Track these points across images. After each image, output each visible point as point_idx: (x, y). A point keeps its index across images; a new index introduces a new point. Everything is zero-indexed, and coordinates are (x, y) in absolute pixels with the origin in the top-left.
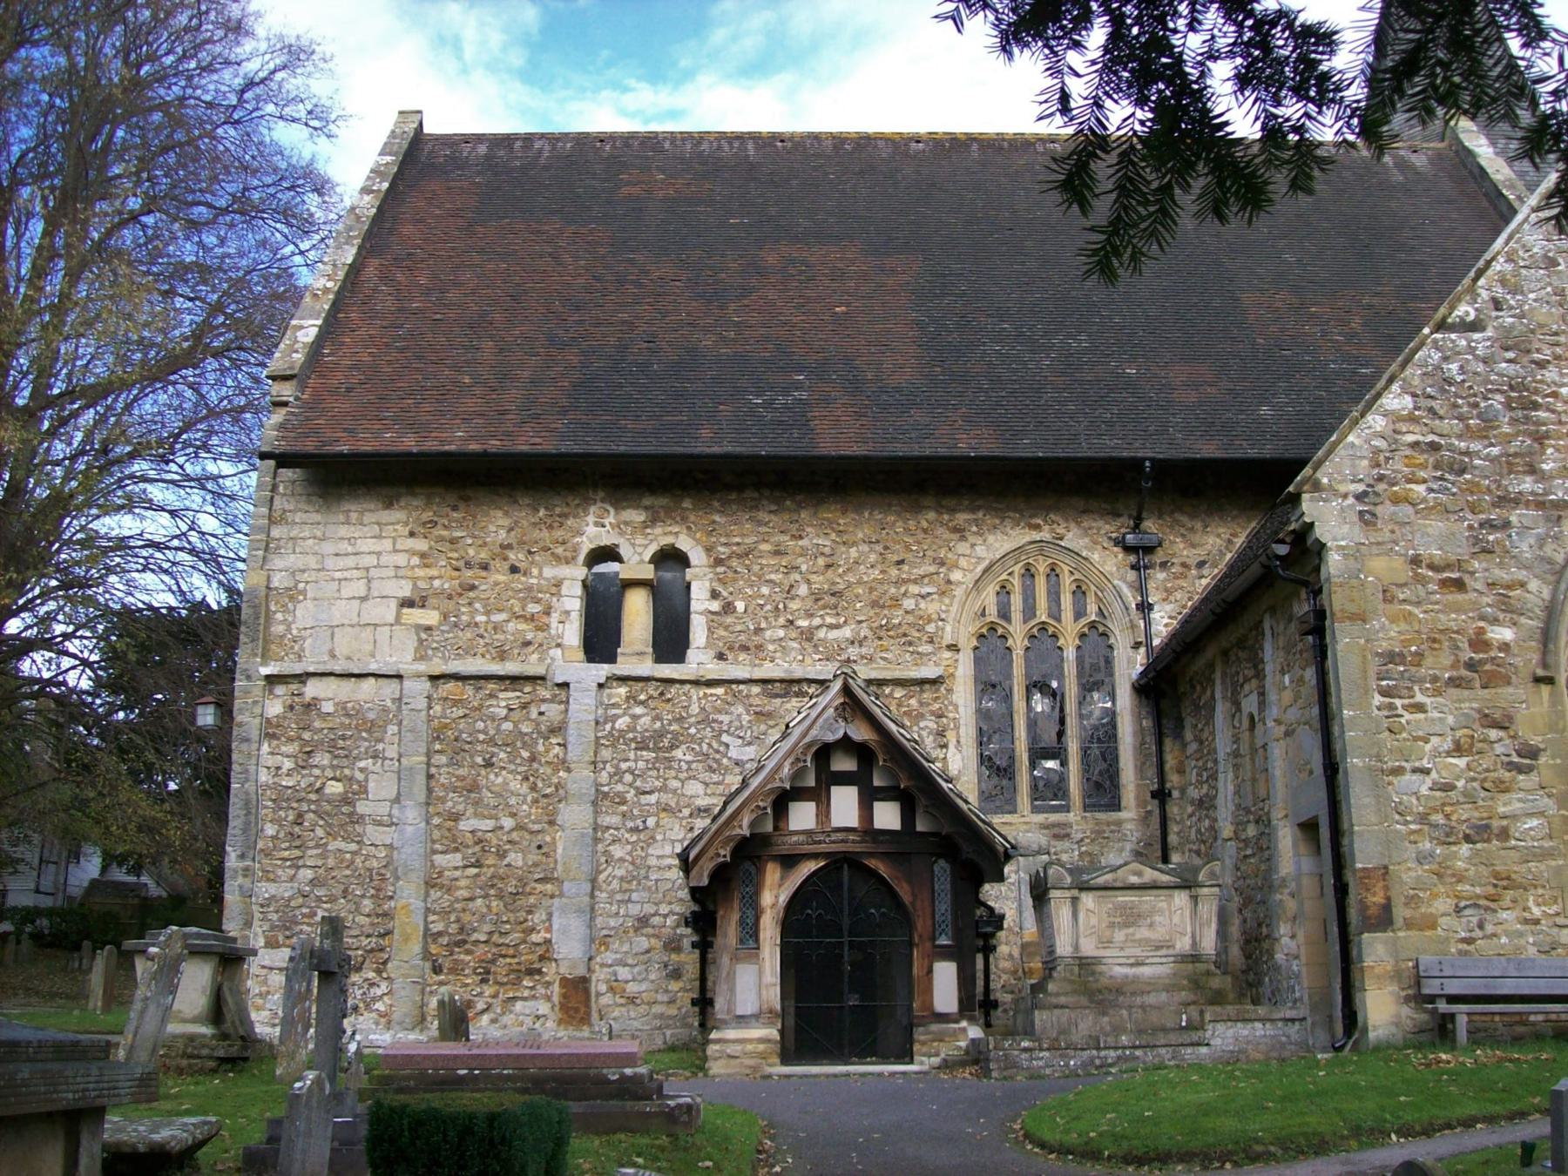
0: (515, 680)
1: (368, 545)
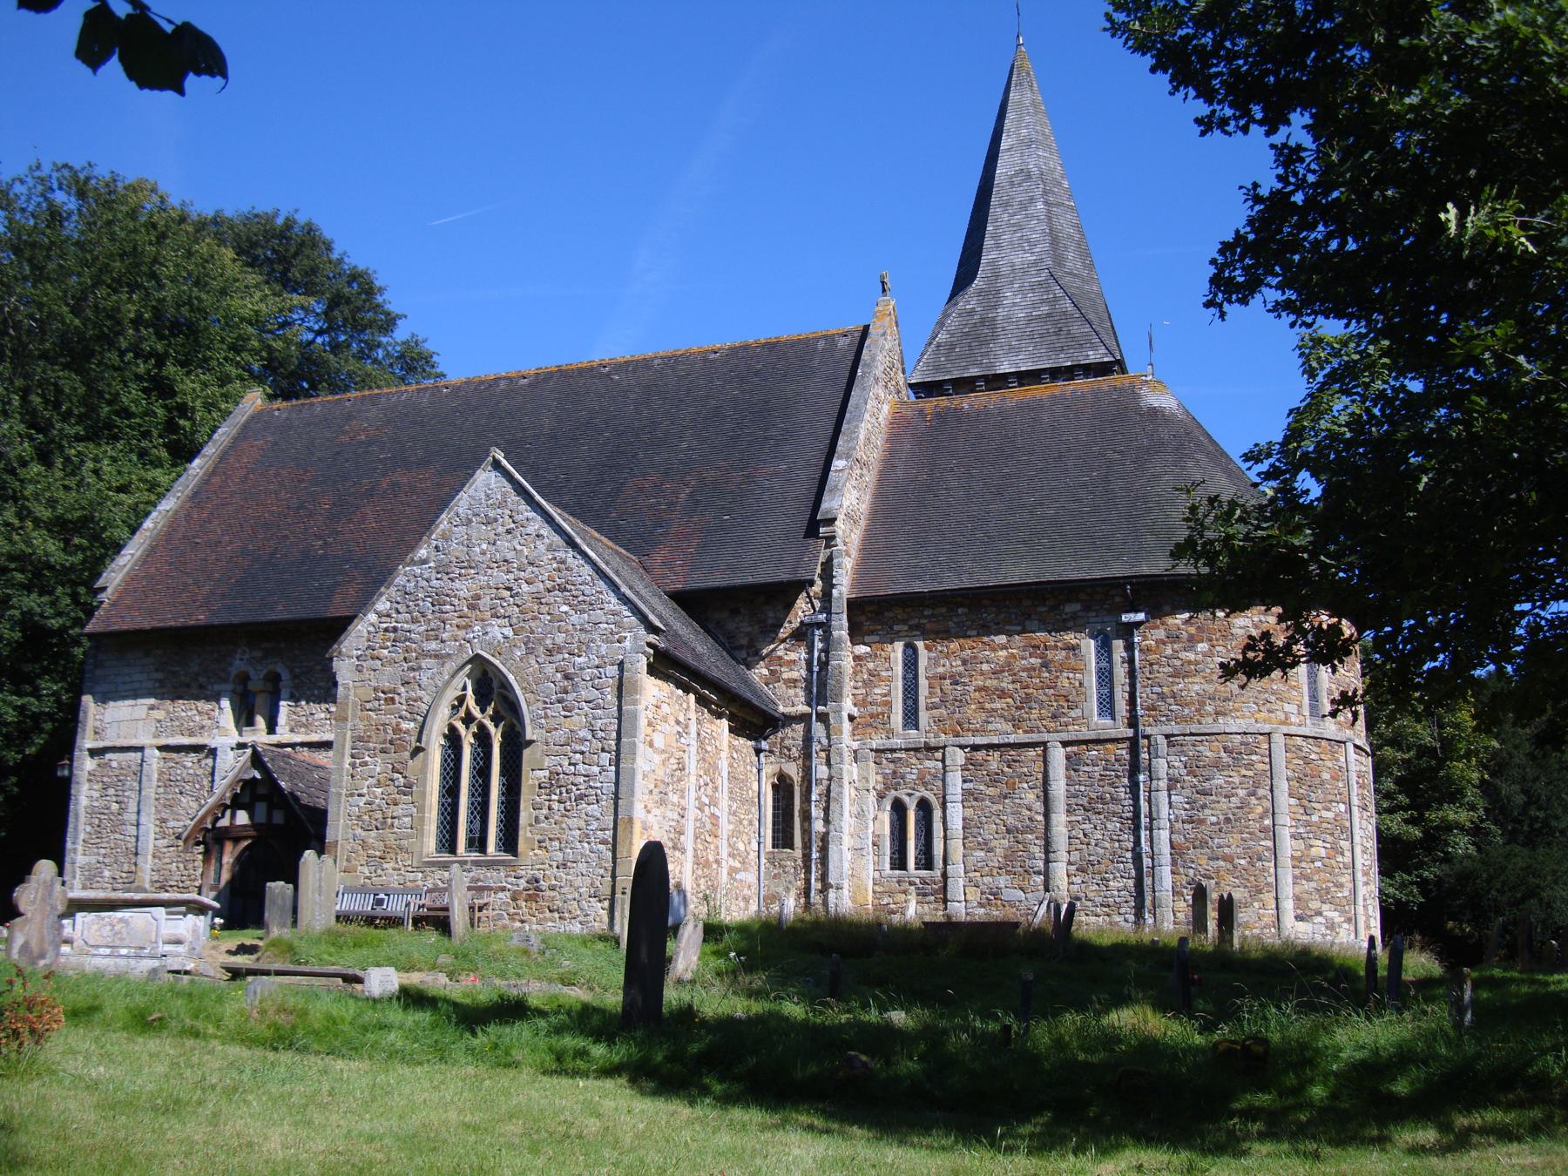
1: (137, 677)
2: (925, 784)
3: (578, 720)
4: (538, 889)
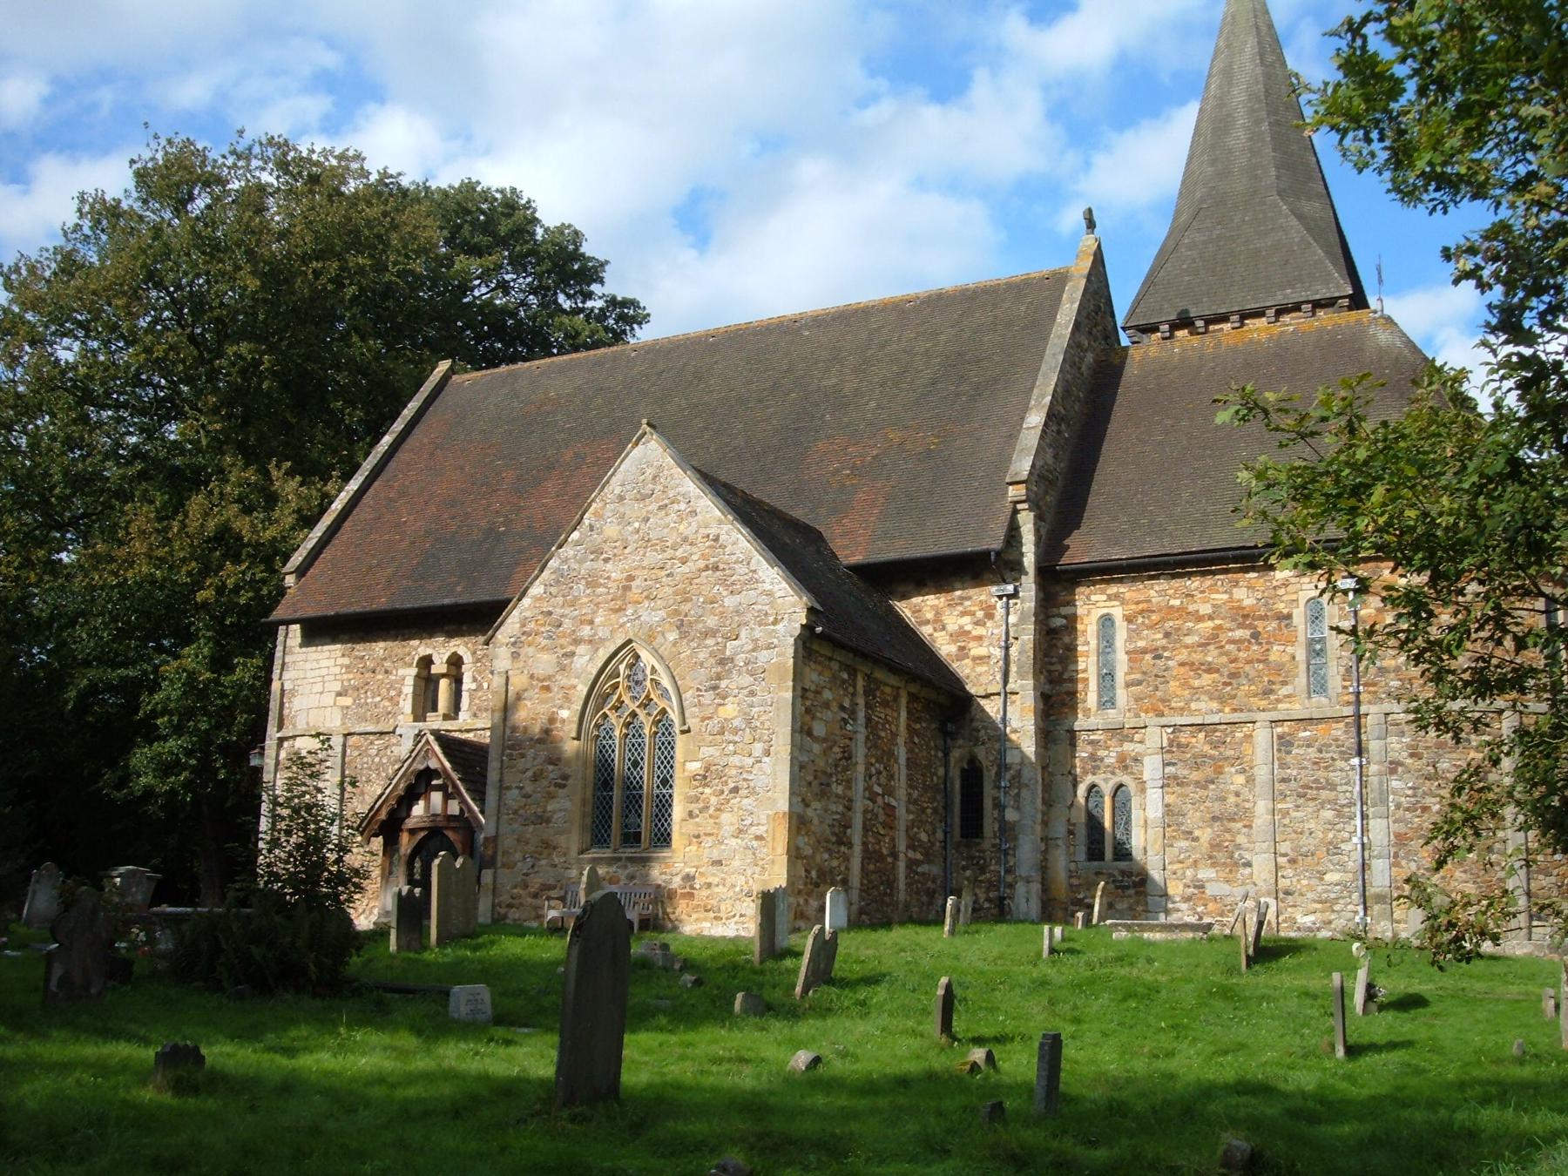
0: (382, 733)
1: (324, 663)
2: (1126, 767)
3: (730, 710)
4: (692, 887)
